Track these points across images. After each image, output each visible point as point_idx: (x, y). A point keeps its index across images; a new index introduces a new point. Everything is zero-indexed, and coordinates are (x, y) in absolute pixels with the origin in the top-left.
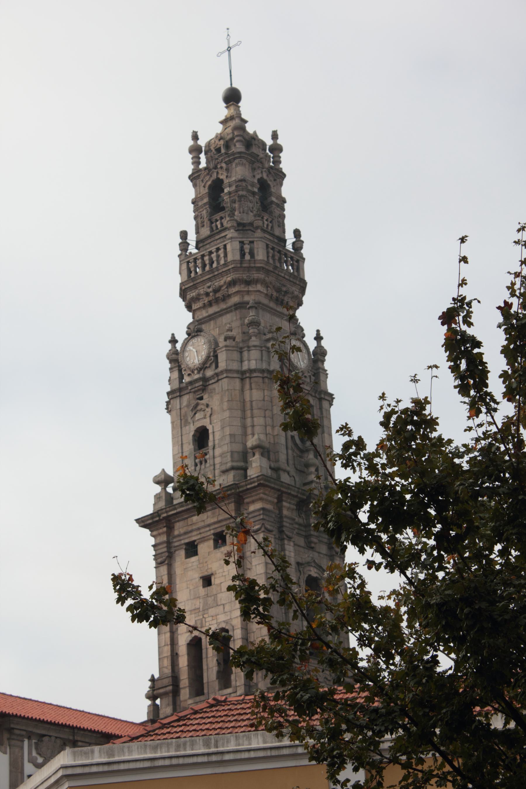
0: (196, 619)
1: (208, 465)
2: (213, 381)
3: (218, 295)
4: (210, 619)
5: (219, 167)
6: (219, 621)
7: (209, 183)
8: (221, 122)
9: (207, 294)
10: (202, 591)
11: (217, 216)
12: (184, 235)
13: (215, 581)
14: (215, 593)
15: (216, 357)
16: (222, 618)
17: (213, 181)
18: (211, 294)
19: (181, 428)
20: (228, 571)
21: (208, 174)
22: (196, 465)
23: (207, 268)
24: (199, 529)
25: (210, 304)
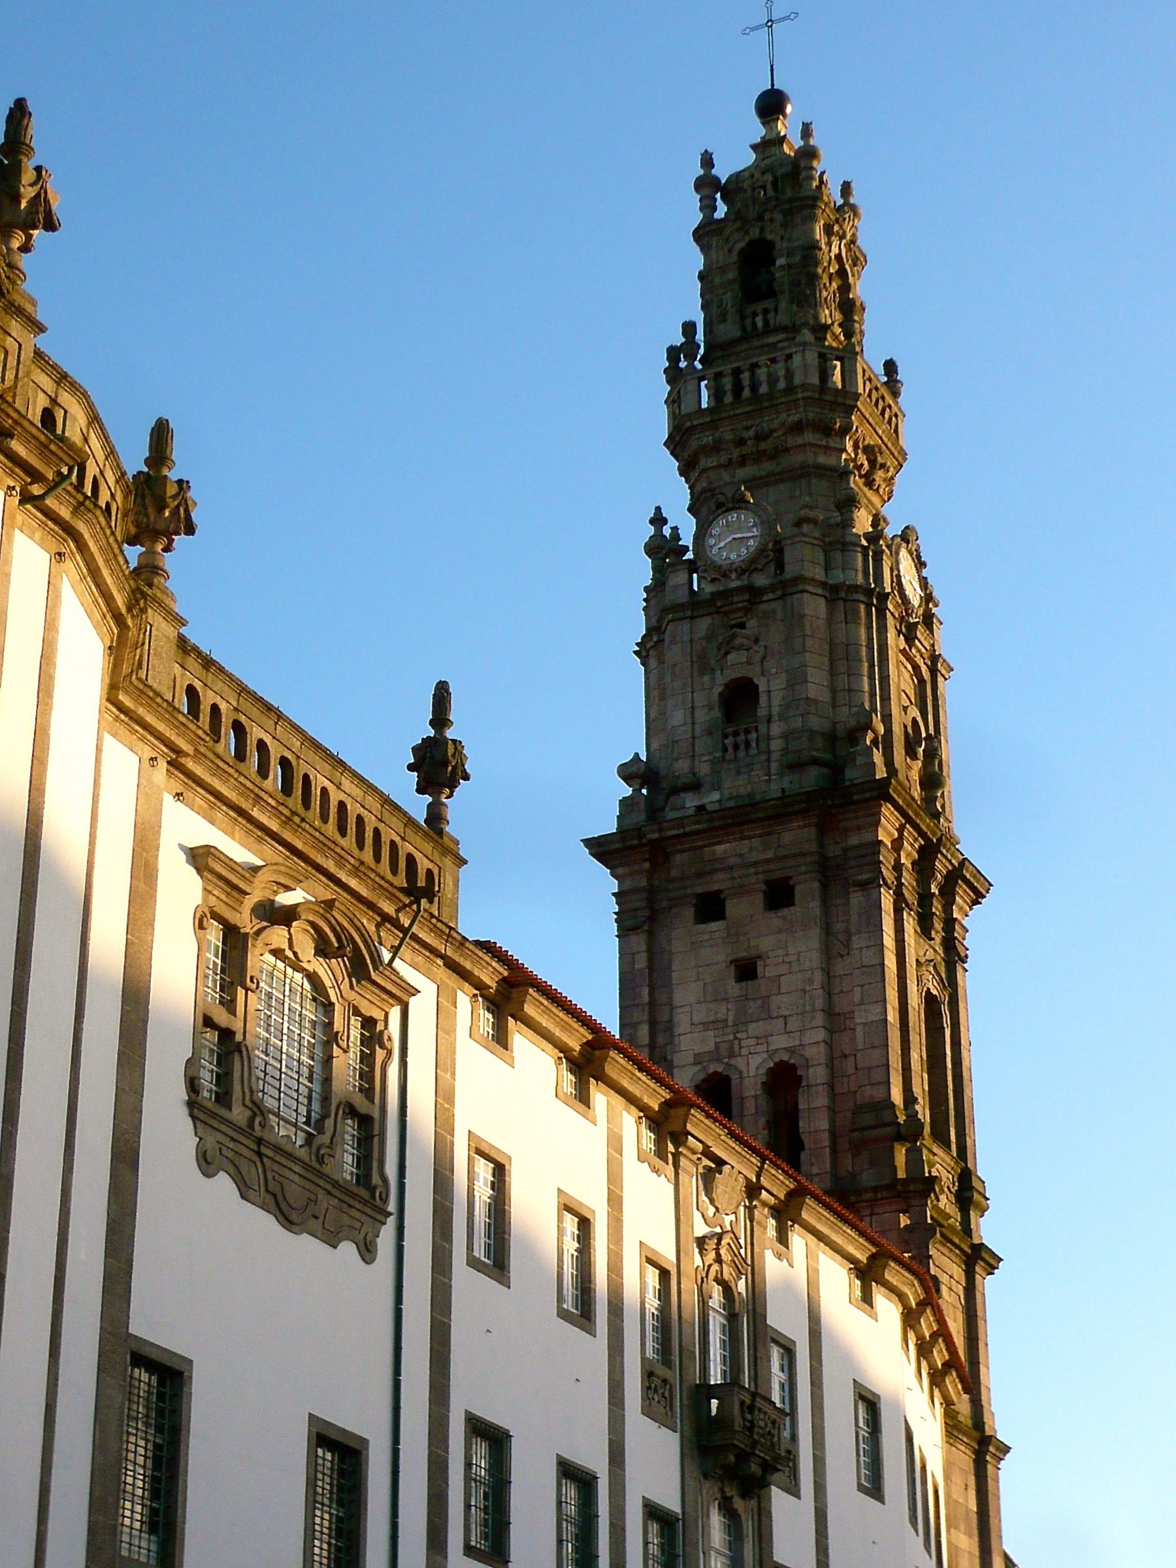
0: (718, 1040)
1: (753, 751)
2: (771, 596)
3: (763, 446)
4: (753, 1041)
5: (767, 216)
6: (772, 1048)
7: (741, 245)
8: (754, 147)
9: (741, 442)
10: (733, 988)
11: (759, 307)
12: (689, 328)
13: (767, 970)
14: (763, 993)
15: (779, 551)
16: (781, 1042)
17: (751, 243)
18: (750, 442)
19: (692, 677)
20: (799, 953)
21: (738, 229)
22: (725, 750)
23: (746, 393)
24: (731, 868)
25: (743, 461)
